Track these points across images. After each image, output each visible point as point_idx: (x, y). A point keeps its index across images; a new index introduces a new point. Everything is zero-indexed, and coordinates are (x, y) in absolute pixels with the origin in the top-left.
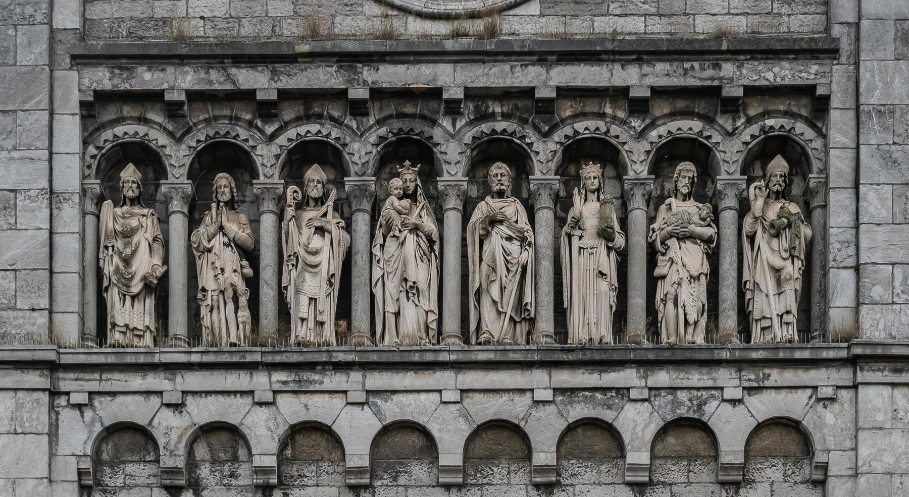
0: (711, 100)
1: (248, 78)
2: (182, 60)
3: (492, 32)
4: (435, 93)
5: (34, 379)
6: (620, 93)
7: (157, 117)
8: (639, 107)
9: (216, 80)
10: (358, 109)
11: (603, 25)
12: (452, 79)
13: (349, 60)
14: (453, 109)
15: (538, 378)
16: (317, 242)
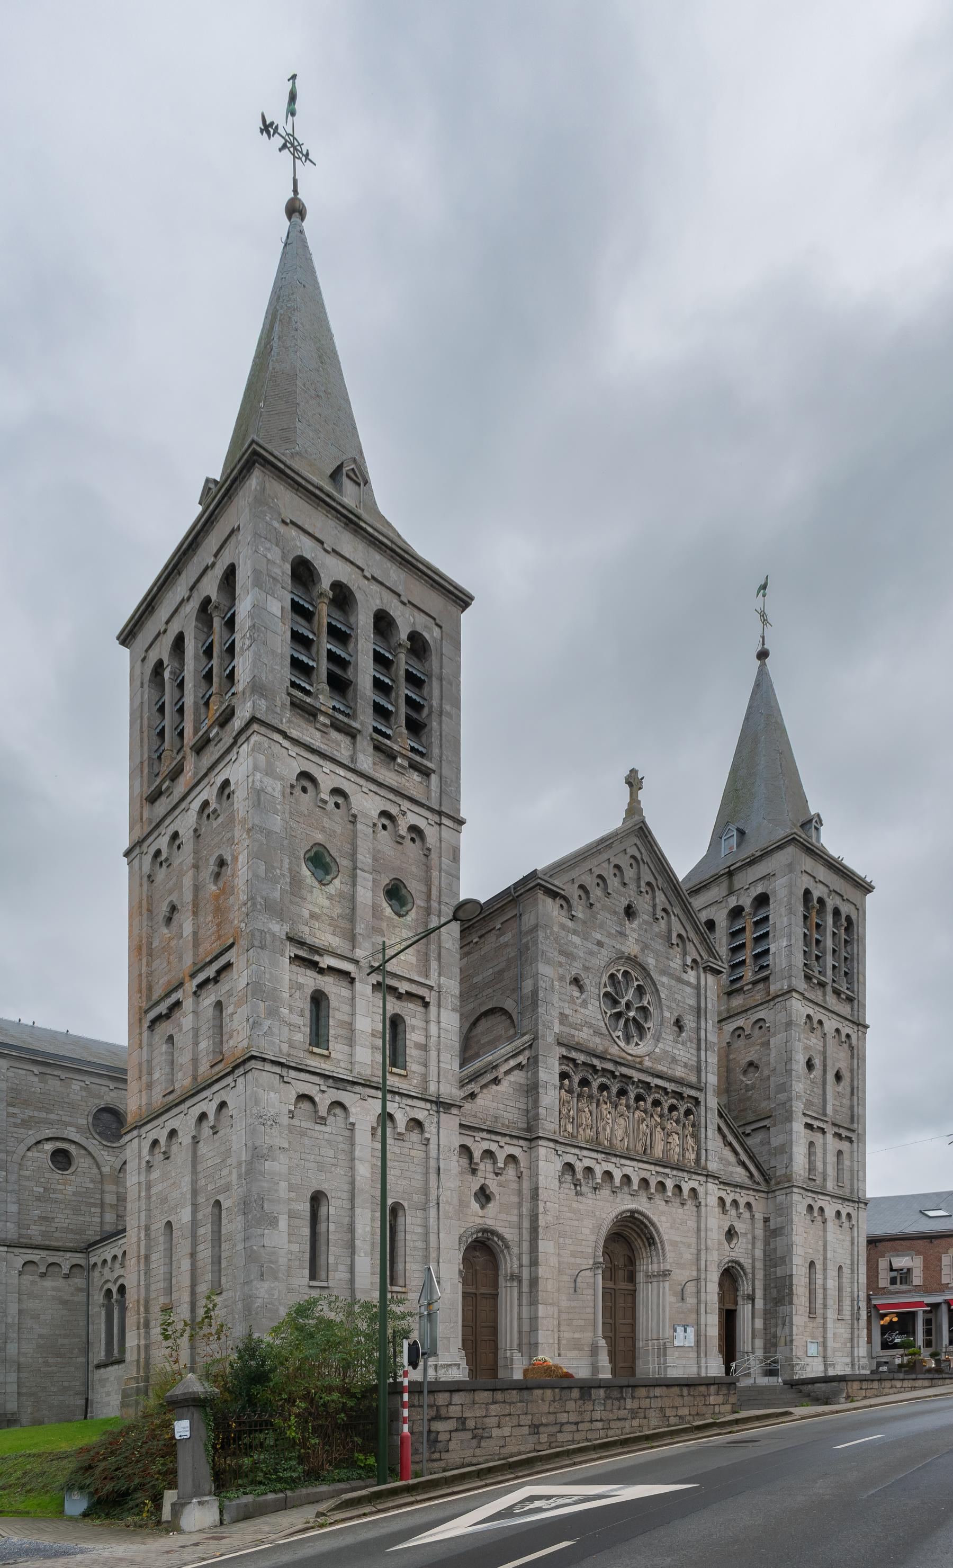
0: (680, 1096)
1: (596, 1062)
2: (582, 1051)
3: (641, 1063)
4: (631, 1078)
5: (551, 1145)
6: (665, 1089)
7: (571, 1066)
8: (667, 1093)
9: (589, 1060)
10: (614, 1077)
11: (660, 1068)
12: (636, 1076)
13: (616, 1063)
14: (633, 1083)
15: (652, 1167)
16: (609, 1116)
